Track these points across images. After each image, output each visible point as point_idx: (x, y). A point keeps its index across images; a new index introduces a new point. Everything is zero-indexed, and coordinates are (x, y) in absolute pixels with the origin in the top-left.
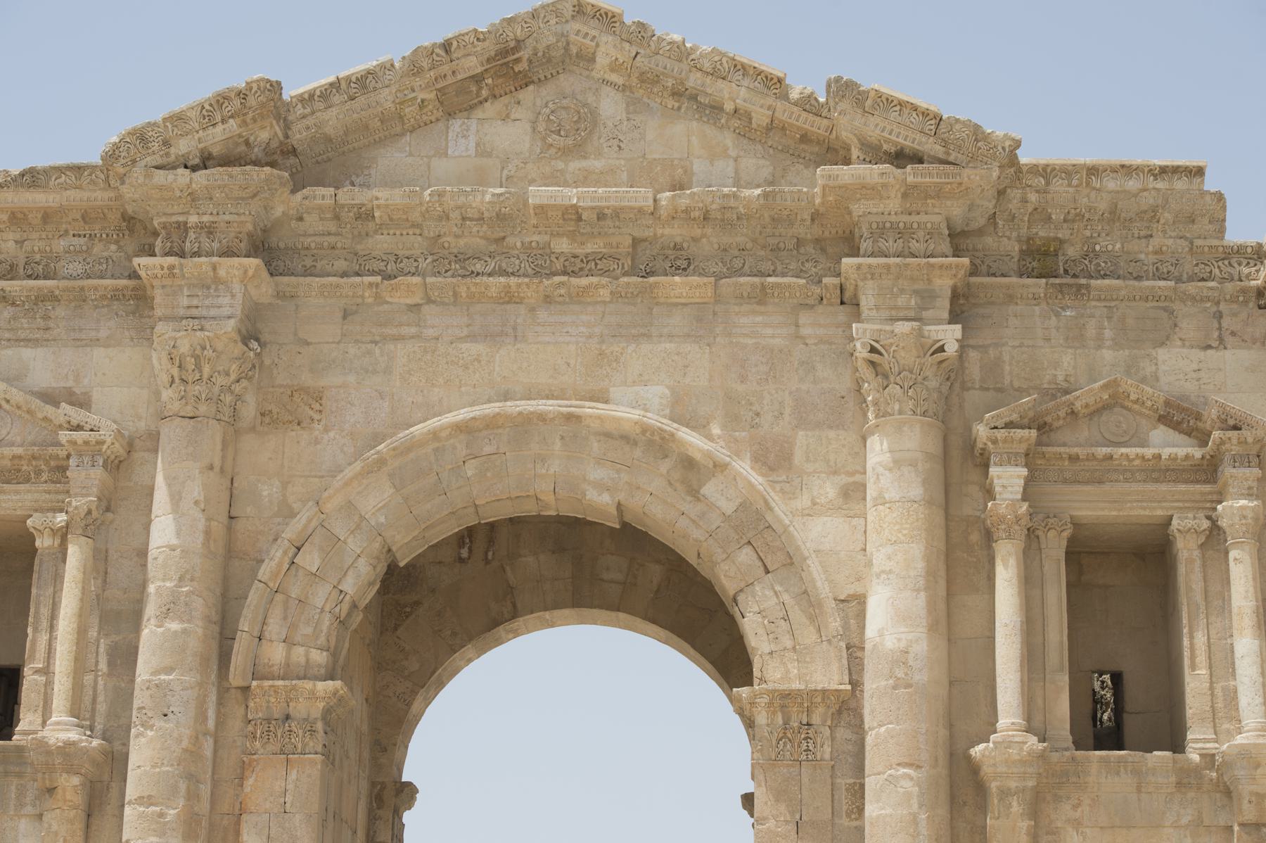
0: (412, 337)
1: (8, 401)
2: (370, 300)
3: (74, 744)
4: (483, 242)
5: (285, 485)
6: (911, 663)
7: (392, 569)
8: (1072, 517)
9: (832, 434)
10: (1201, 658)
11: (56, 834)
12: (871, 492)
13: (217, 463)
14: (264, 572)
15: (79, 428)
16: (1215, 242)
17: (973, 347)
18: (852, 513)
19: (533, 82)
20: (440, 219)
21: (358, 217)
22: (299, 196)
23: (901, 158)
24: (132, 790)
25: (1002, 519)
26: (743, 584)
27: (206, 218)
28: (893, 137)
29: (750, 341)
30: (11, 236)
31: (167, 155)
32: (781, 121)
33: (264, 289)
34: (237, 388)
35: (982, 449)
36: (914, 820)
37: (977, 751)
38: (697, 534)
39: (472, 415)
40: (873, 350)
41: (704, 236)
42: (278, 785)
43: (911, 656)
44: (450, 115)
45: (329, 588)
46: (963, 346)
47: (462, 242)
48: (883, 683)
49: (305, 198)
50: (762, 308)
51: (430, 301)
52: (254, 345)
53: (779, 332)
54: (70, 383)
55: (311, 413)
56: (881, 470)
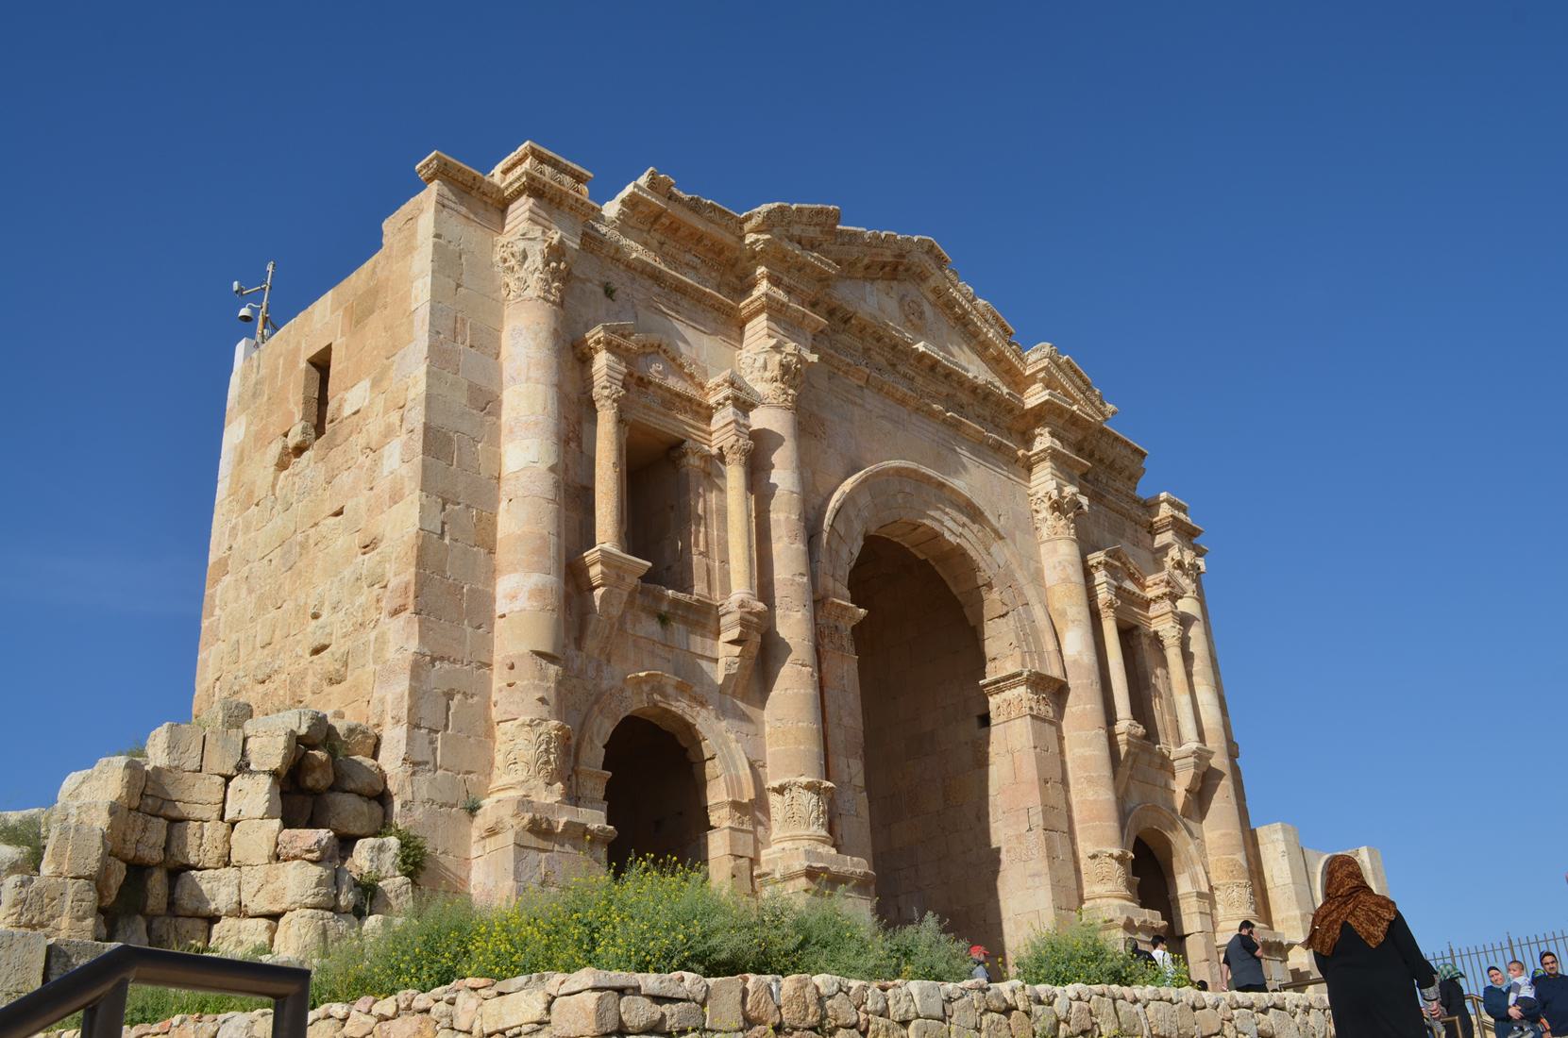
0: (860, 405)
1: (665, 351)
4: (885, 363)
11: (733, 674)
27: (792, 282)
31: (788, 231)
39: (906, 466)
41: (972, 404)
44: (865, 279)
48: (1085, 681)
50: (995, 456)
51: (867, 388)
54: (694, 356)
55: (820, 432)
56: (1067, 564)
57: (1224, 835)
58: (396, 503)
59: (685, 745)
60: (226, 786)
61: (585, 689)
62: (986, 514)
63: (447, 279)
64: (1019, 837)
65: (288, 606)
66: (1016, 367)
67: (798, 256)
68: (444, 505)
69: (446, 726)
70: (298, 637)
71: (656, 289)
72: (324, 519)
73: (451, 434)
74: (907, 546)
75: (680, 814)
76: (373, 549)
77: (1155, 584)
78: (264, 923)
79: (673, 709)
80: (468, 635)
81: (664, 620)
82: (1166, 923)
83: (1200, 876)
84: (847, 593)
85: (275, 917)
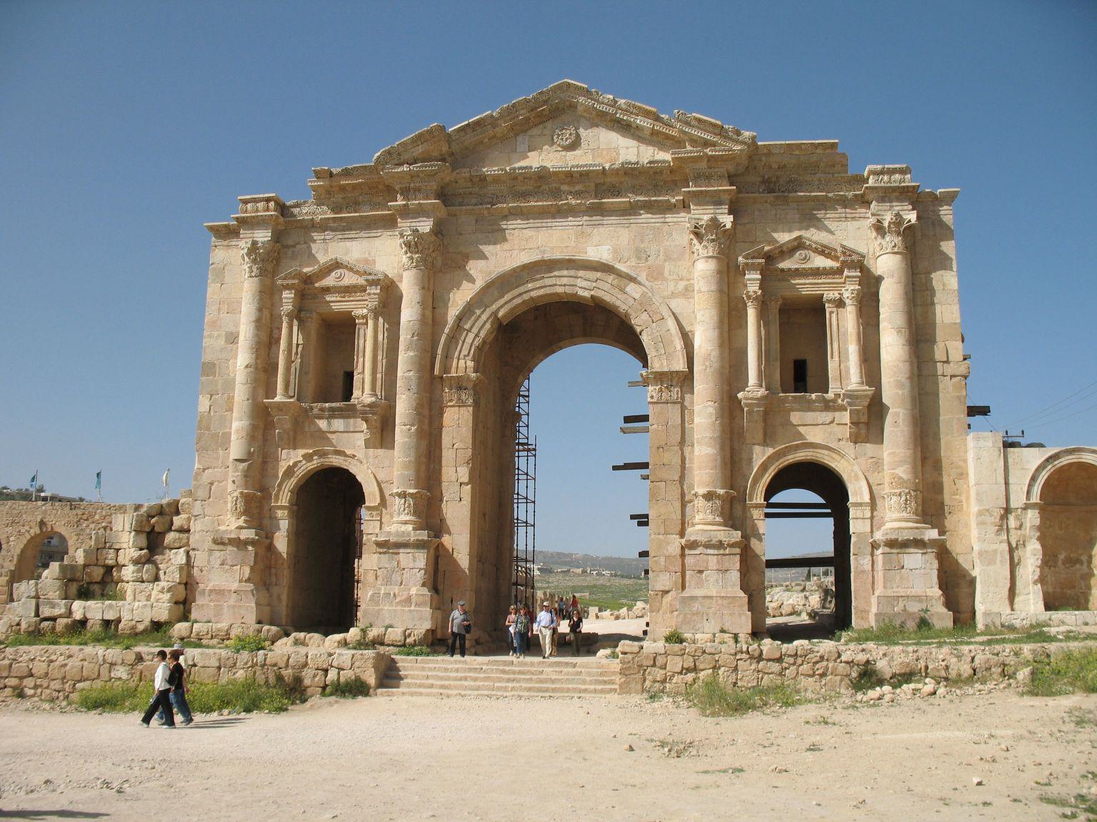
1: (342, 264)
2: (487, 215)
3: (374, 402)
6: (712, 359)
7: (500, 325)
8: (782, 296)
10: (836, 354)
12: (696, 288)
13: (426, 286)
14: (447, 330)
15: (370, 274)
16: (843, 175)
17: (740, 224)
18: (688, 297)
19: (551, 118)
21: (481, 180)
22: (455, 173)
24: (398, 420)
25: (749, 297)
29: (646, 225)
30: (341, 196)
33: (442, 212)
34: (433, 255)
36: (714, 423)
37: (740, 395)
40: (696, 227)
42: (456, 417)
43: (712, 356)
44: (517, 135)
45: (473, 335)
46: (734, 223)
47: (524, 188)
48: (701, 368)
49: (457, 174)
52: (439, 236)
53: (657, 220)
54: (367, 256)
56: (700, 278)
57: (890, 454)
62: (616, 266)
68: (211, 396)
69: (210, 497)
83: (864, 489)
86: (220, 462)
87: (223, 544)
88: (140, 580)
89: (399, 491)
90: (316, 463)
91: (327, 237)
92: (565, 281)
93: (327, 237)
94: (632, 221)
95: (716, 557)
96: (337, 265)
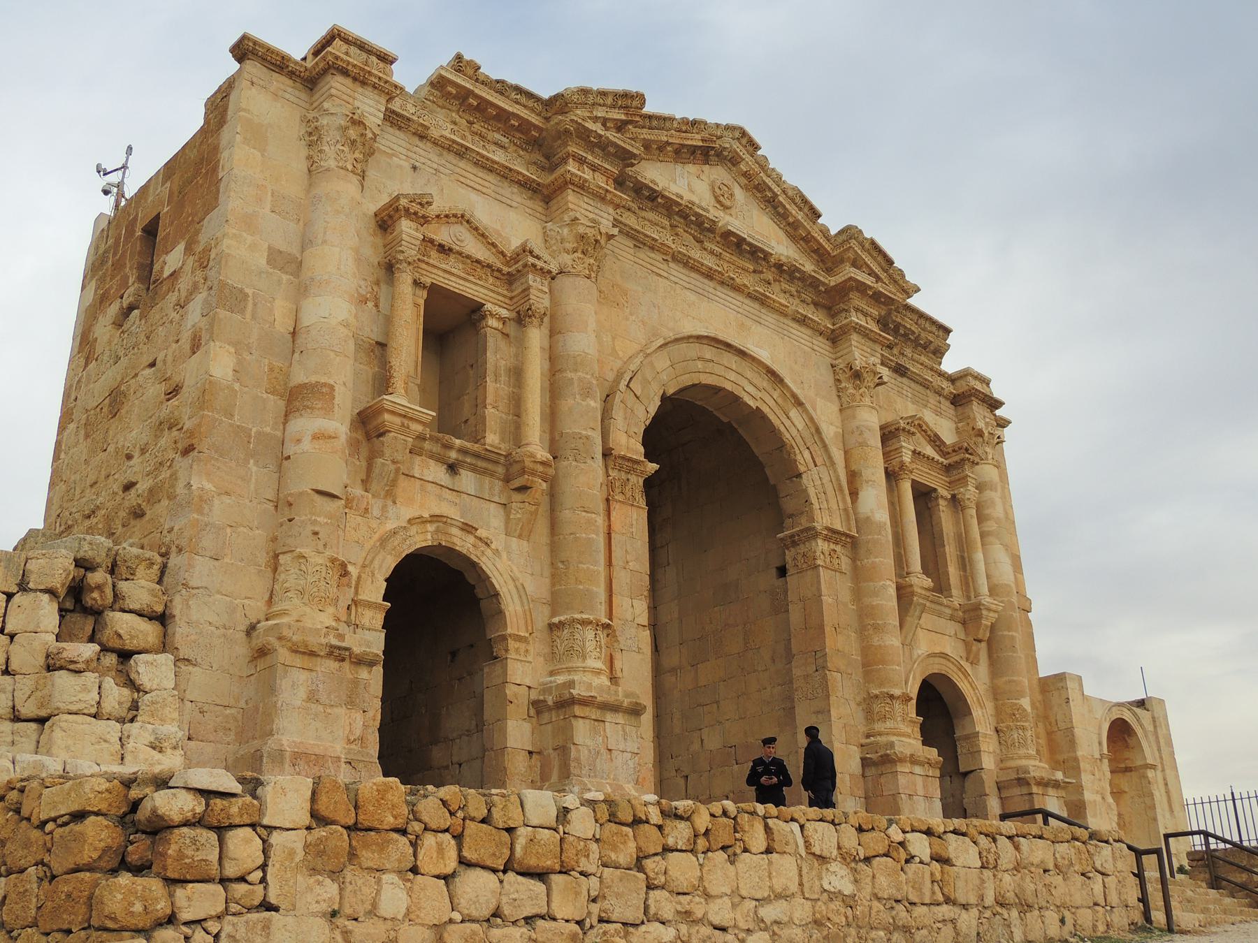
5: (614, 338)
9: (829, 404)
11: (519, 519)
15: (538, 258)
16: (936, 366)
20: (681, 216)
23: (878, 279)
26: (806, 469)
27: (596, 161)
28: (872, 265)
29: (798, 344)
32: (813, 237)
35: (890, 432)
38: (788, 436)
54: (499, 227)
58: (194, 353)
59: (473, 583)
60: (8, 601)
61: (370, 527)
62: (786, 380)
63: (252, 150)
64: (806, 677)
65: (111, 449)
66: (823, 247)
67: (601, 136)
70: (116, 477)
71: (462, 164)
72: (143, 369)
73: (247, 290)
74: (710, 409)
75: (472, 646)
76: (175, 396)
77: (954, 451)
78: (33, 726)
79: (457, 548)
80: (254, 474)
81: (452, 468)
82: (941, 759)
84: (642, 449)
85: (42, 721)
86: (252, 487)
87: (312, 654)
88: (93, 710)
89: (591, 618)
90: (421, 539)
91: (442, 169)
92: (732, 376)
93: (442, 169)
94: (785, 332)
95: (921, 778)
96: (463, 219)
